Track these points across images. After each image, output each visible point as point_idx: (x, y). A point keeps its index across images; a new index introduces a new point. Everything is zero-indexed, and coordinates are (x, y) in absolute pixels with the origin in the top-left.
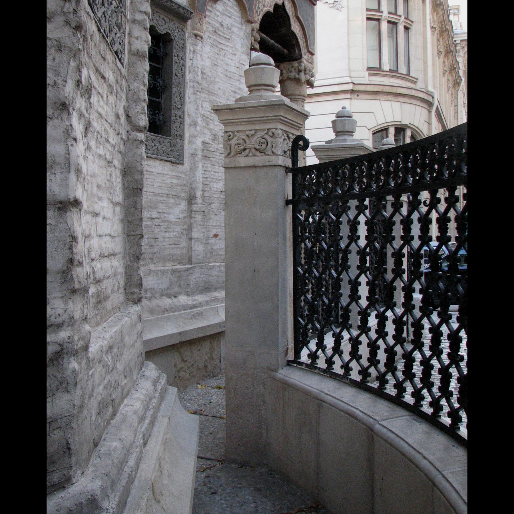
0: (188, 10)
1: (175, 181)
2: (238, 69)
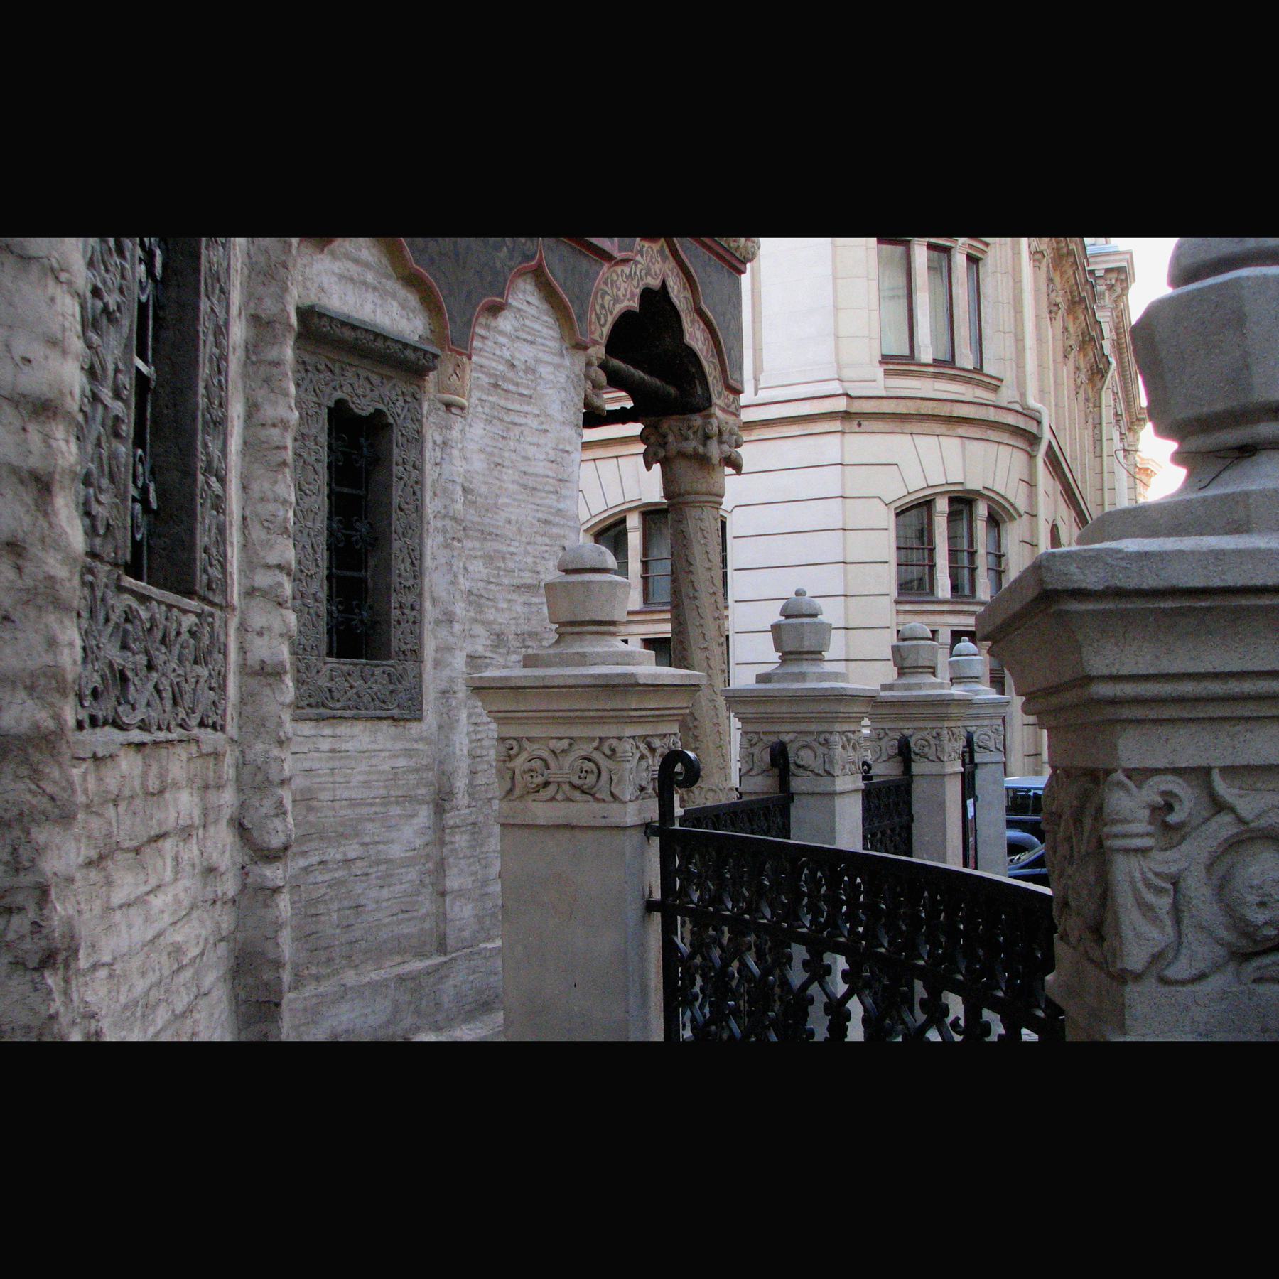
0: (426, 352)
1: (402, 762)
2: (554, 465)
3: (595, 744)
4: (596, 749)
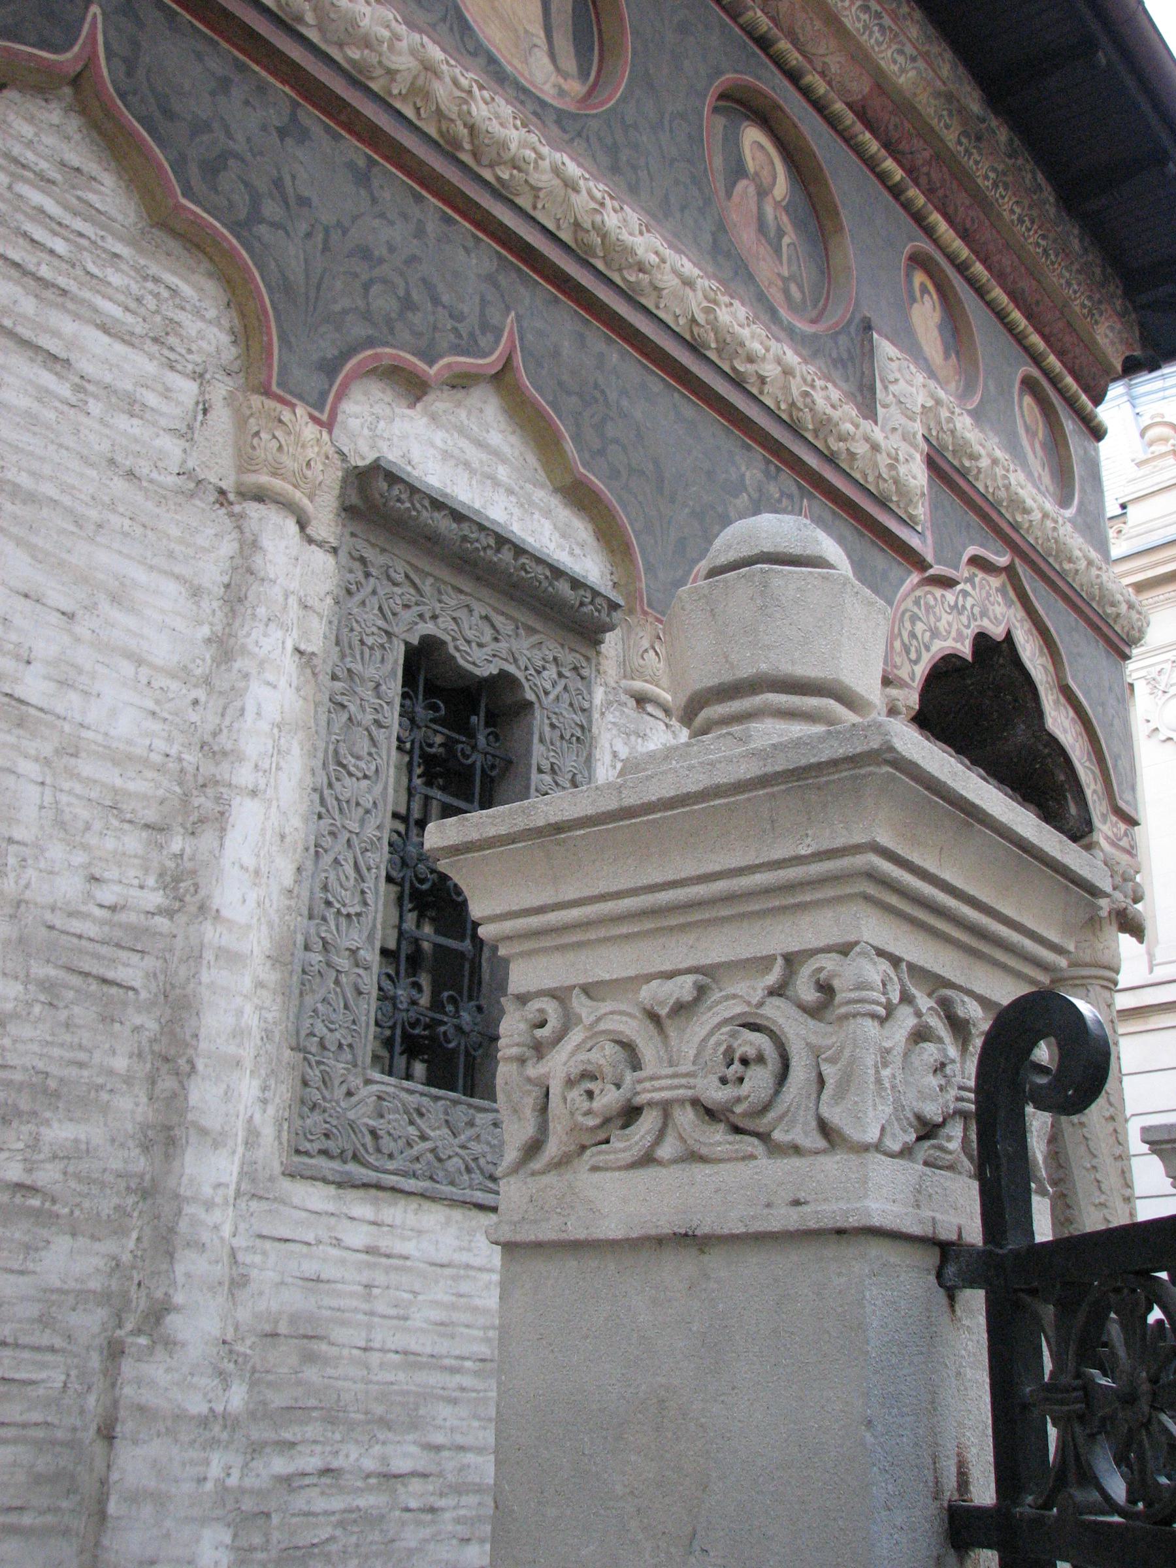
3: (773, 978)
4: (774, 992)
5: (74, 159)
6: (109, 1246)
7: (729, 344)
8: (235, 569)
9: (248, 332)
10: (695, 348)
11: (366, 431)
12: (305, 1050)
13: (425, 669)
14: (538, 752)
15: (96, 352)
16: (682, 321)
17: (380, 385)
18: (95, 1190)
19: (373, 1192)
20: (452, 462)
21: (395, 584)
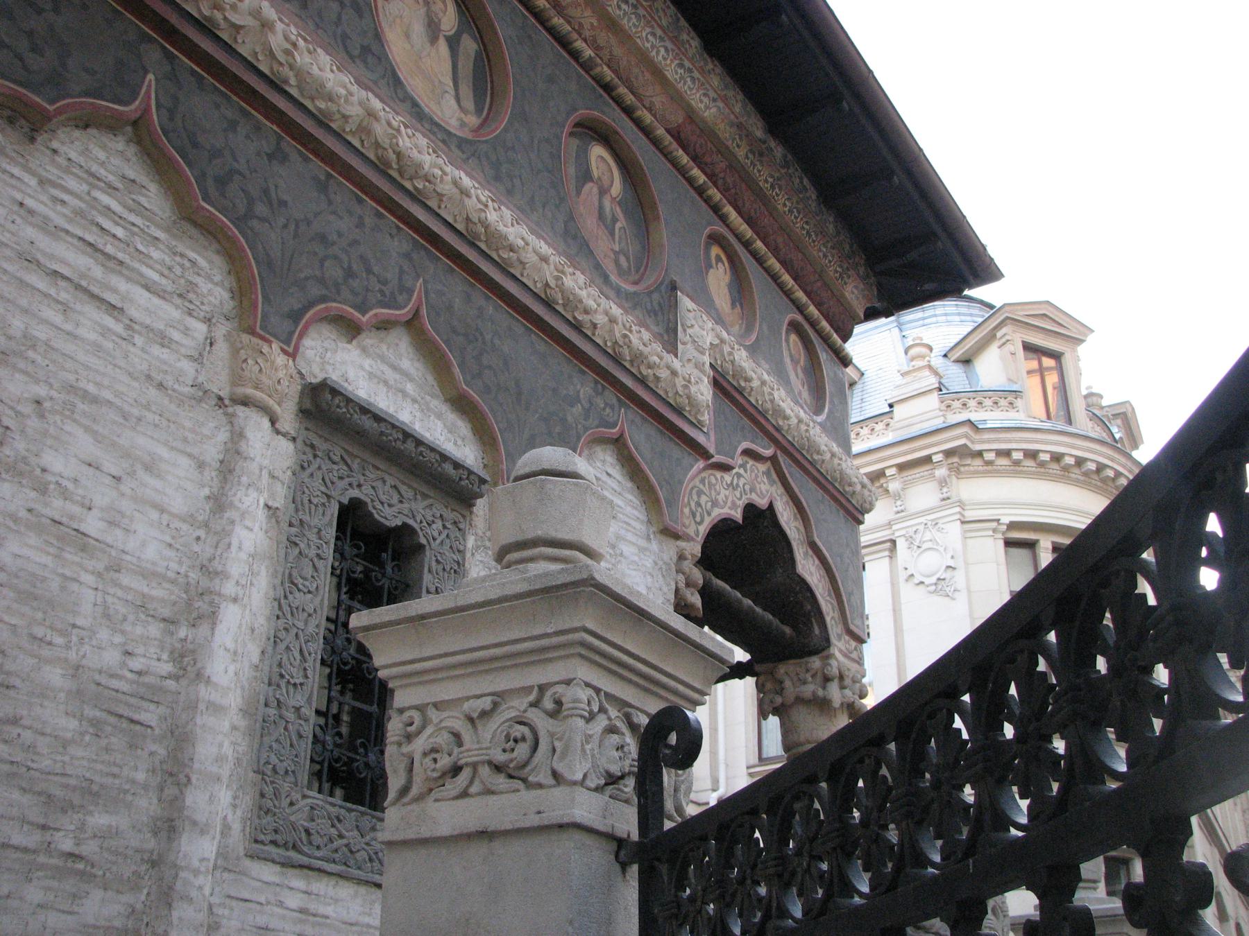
5: (131, 174)
6: (128, 898)
7: (572, 302)
8: (227, 451)
9: (242, 292)
10: (548, 304)
11: (318, 359)
12: (264, 774)
13: (352, 519)
14: (427, 578)
15: (141, 303)
16: (539, 285)
17: (329, 327)
18: (120, 861)
19: (306, 871)
20: (376, 380)
21: (334, 463)
